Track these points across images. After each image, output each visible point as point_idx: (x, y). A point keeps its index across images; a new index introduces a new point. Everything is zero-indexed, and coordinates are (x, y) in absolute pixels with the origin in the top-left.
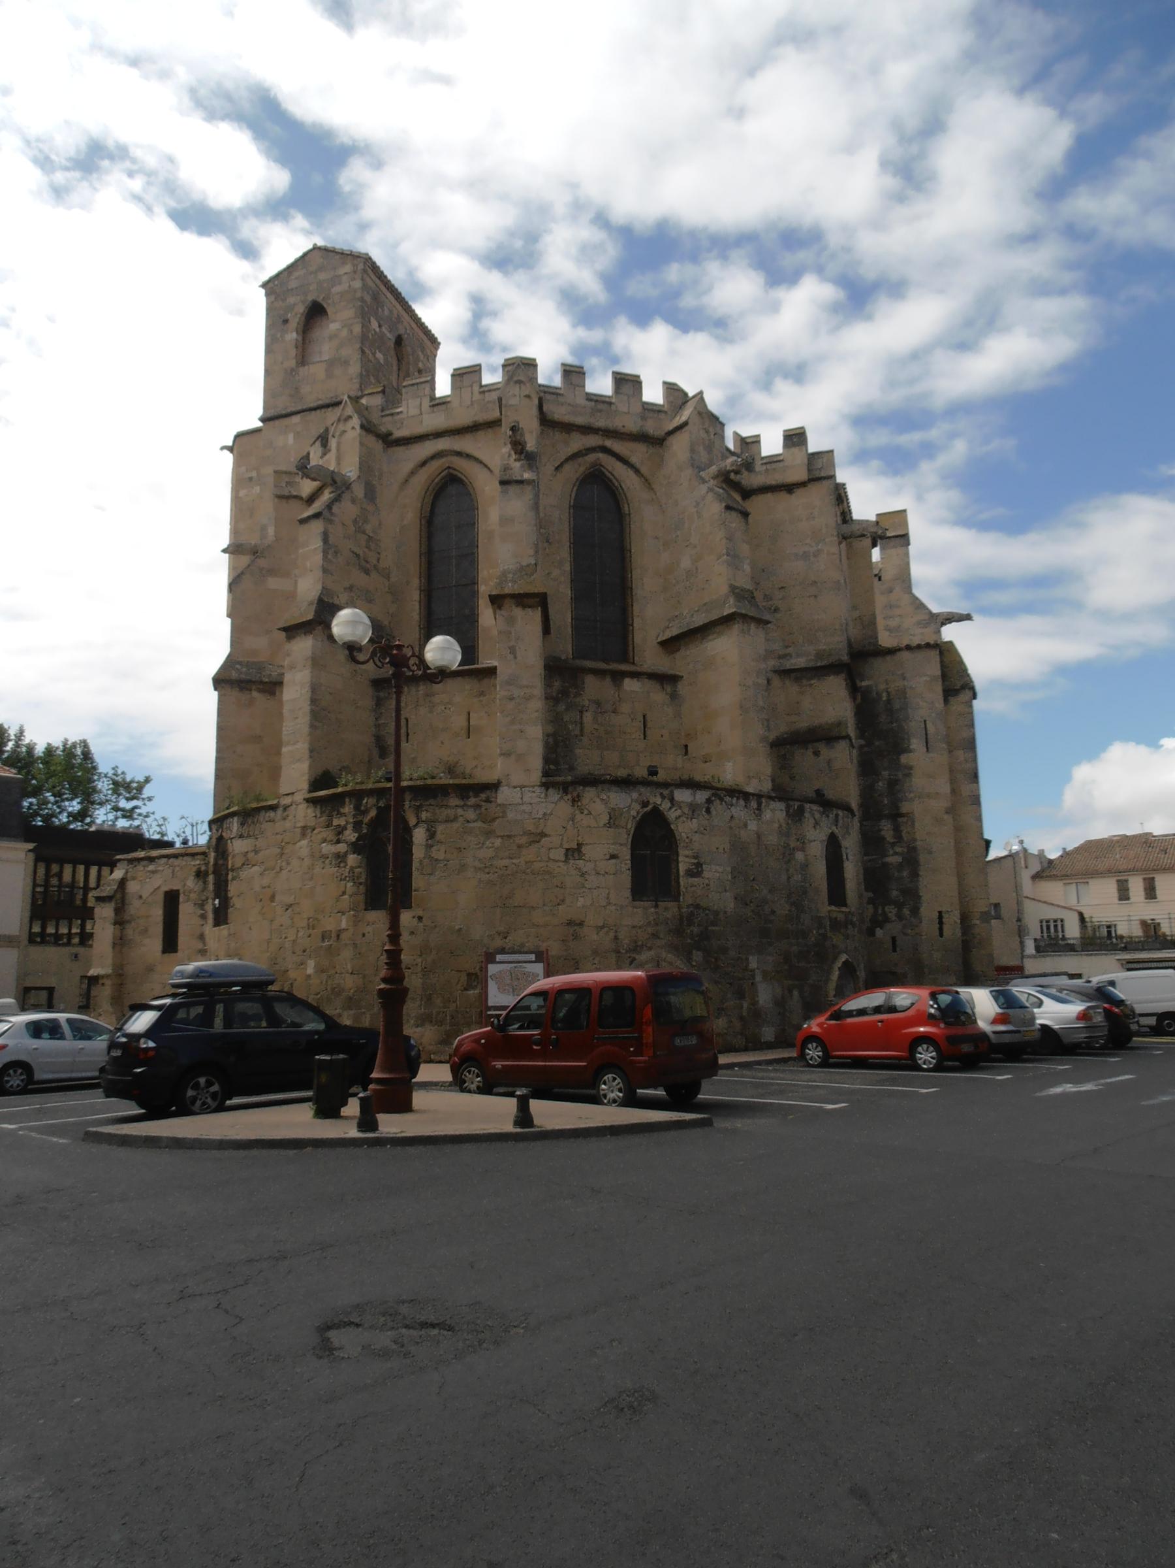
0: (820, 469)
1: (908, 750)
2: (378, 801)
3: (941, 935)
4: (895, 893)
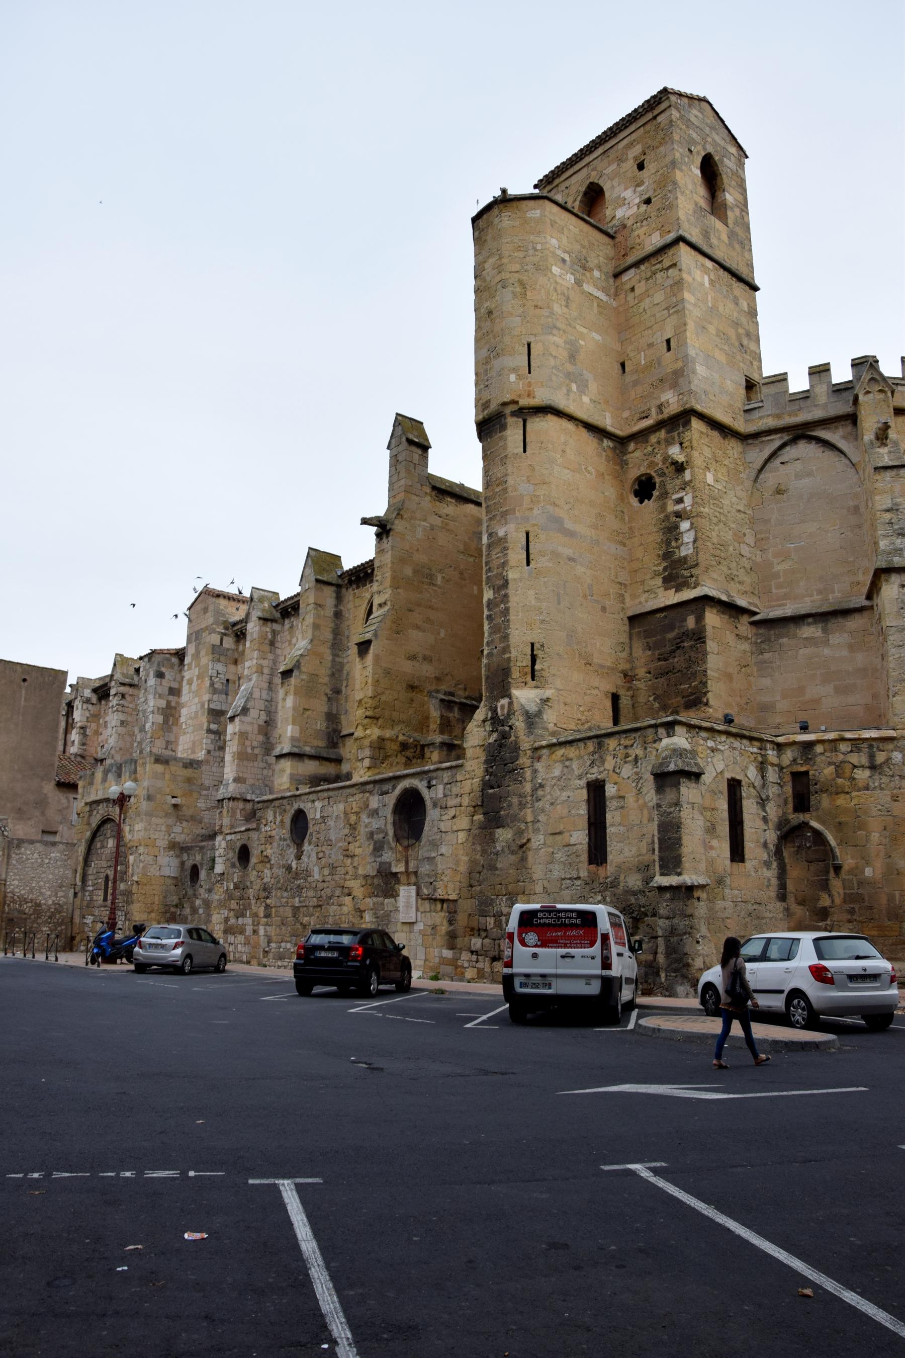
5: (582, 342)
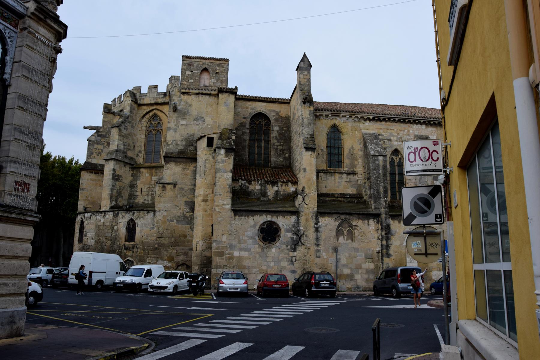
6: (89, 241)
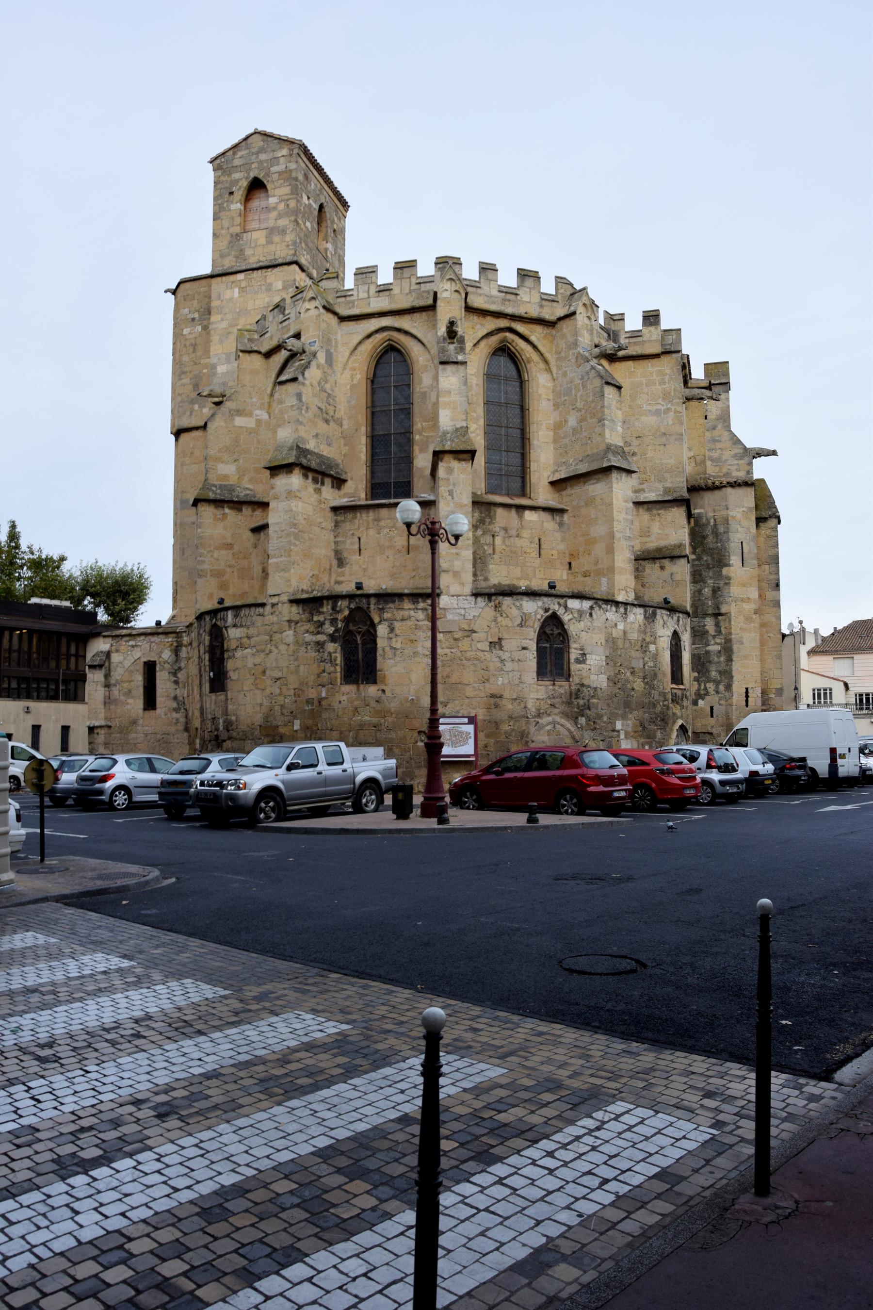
0: (670, 345)
1: (728, 565)
2: (349, 604)
3: (747, 706)
4: (713, 674)
5: (205, 371)
6: (593, 677)
